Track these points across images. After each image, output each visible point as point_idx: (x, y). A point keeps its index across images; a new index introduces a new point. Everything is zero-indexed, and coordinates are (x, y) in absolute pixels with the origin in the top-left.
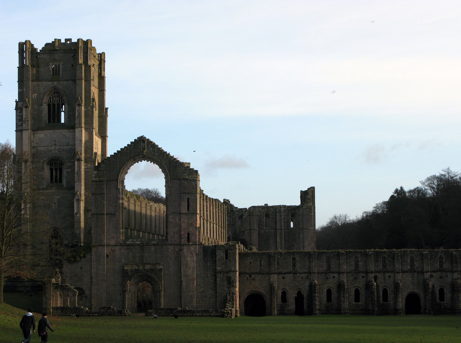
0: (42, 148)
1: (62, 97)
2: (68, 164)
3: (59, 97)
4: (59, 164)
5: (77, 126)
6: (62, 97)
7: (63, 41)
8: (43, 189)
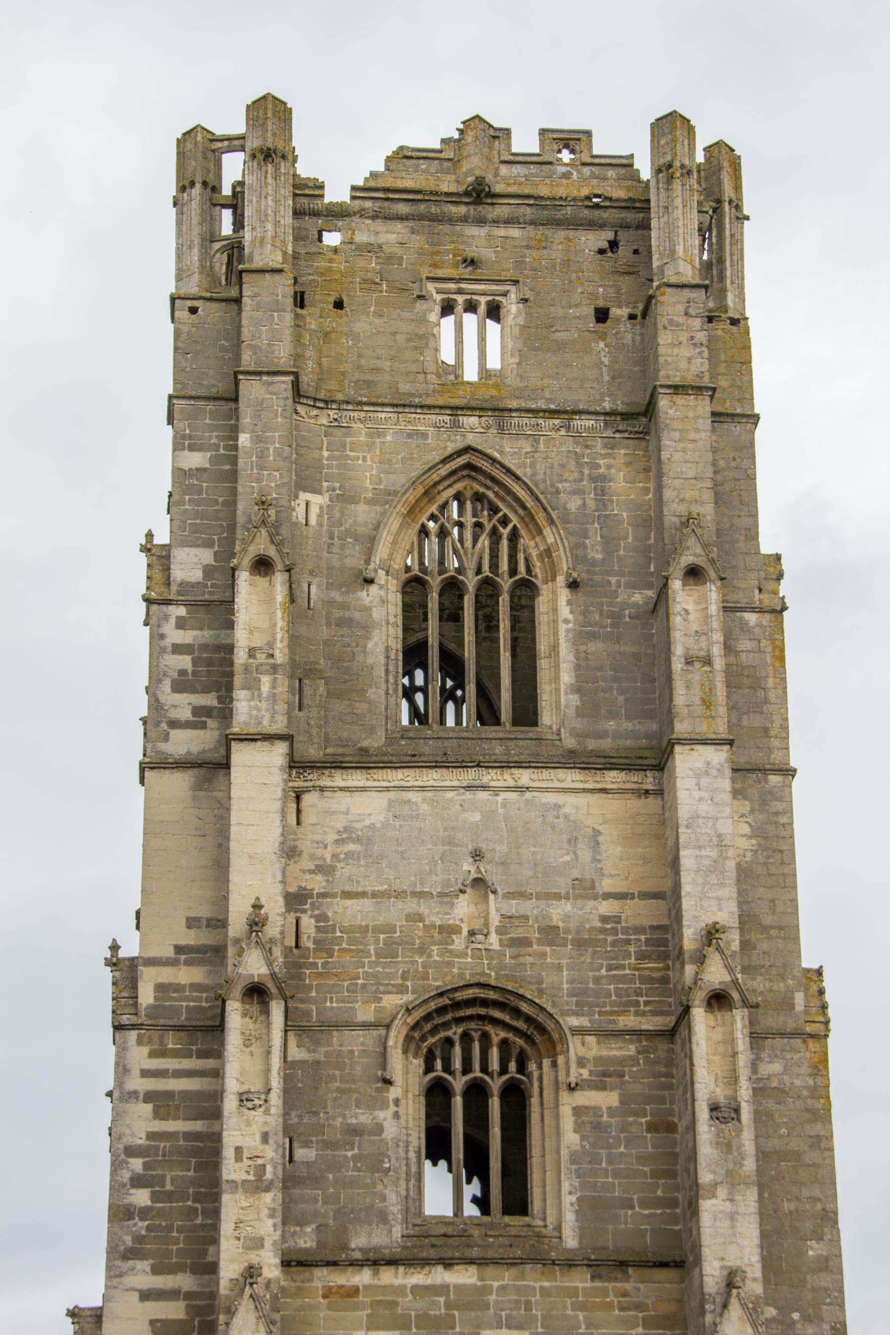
0: (366, 904)
1: (514, 536)
3: (495, 535)
5: (681, 728)
7: (525, 142)
8: (376, 1261)
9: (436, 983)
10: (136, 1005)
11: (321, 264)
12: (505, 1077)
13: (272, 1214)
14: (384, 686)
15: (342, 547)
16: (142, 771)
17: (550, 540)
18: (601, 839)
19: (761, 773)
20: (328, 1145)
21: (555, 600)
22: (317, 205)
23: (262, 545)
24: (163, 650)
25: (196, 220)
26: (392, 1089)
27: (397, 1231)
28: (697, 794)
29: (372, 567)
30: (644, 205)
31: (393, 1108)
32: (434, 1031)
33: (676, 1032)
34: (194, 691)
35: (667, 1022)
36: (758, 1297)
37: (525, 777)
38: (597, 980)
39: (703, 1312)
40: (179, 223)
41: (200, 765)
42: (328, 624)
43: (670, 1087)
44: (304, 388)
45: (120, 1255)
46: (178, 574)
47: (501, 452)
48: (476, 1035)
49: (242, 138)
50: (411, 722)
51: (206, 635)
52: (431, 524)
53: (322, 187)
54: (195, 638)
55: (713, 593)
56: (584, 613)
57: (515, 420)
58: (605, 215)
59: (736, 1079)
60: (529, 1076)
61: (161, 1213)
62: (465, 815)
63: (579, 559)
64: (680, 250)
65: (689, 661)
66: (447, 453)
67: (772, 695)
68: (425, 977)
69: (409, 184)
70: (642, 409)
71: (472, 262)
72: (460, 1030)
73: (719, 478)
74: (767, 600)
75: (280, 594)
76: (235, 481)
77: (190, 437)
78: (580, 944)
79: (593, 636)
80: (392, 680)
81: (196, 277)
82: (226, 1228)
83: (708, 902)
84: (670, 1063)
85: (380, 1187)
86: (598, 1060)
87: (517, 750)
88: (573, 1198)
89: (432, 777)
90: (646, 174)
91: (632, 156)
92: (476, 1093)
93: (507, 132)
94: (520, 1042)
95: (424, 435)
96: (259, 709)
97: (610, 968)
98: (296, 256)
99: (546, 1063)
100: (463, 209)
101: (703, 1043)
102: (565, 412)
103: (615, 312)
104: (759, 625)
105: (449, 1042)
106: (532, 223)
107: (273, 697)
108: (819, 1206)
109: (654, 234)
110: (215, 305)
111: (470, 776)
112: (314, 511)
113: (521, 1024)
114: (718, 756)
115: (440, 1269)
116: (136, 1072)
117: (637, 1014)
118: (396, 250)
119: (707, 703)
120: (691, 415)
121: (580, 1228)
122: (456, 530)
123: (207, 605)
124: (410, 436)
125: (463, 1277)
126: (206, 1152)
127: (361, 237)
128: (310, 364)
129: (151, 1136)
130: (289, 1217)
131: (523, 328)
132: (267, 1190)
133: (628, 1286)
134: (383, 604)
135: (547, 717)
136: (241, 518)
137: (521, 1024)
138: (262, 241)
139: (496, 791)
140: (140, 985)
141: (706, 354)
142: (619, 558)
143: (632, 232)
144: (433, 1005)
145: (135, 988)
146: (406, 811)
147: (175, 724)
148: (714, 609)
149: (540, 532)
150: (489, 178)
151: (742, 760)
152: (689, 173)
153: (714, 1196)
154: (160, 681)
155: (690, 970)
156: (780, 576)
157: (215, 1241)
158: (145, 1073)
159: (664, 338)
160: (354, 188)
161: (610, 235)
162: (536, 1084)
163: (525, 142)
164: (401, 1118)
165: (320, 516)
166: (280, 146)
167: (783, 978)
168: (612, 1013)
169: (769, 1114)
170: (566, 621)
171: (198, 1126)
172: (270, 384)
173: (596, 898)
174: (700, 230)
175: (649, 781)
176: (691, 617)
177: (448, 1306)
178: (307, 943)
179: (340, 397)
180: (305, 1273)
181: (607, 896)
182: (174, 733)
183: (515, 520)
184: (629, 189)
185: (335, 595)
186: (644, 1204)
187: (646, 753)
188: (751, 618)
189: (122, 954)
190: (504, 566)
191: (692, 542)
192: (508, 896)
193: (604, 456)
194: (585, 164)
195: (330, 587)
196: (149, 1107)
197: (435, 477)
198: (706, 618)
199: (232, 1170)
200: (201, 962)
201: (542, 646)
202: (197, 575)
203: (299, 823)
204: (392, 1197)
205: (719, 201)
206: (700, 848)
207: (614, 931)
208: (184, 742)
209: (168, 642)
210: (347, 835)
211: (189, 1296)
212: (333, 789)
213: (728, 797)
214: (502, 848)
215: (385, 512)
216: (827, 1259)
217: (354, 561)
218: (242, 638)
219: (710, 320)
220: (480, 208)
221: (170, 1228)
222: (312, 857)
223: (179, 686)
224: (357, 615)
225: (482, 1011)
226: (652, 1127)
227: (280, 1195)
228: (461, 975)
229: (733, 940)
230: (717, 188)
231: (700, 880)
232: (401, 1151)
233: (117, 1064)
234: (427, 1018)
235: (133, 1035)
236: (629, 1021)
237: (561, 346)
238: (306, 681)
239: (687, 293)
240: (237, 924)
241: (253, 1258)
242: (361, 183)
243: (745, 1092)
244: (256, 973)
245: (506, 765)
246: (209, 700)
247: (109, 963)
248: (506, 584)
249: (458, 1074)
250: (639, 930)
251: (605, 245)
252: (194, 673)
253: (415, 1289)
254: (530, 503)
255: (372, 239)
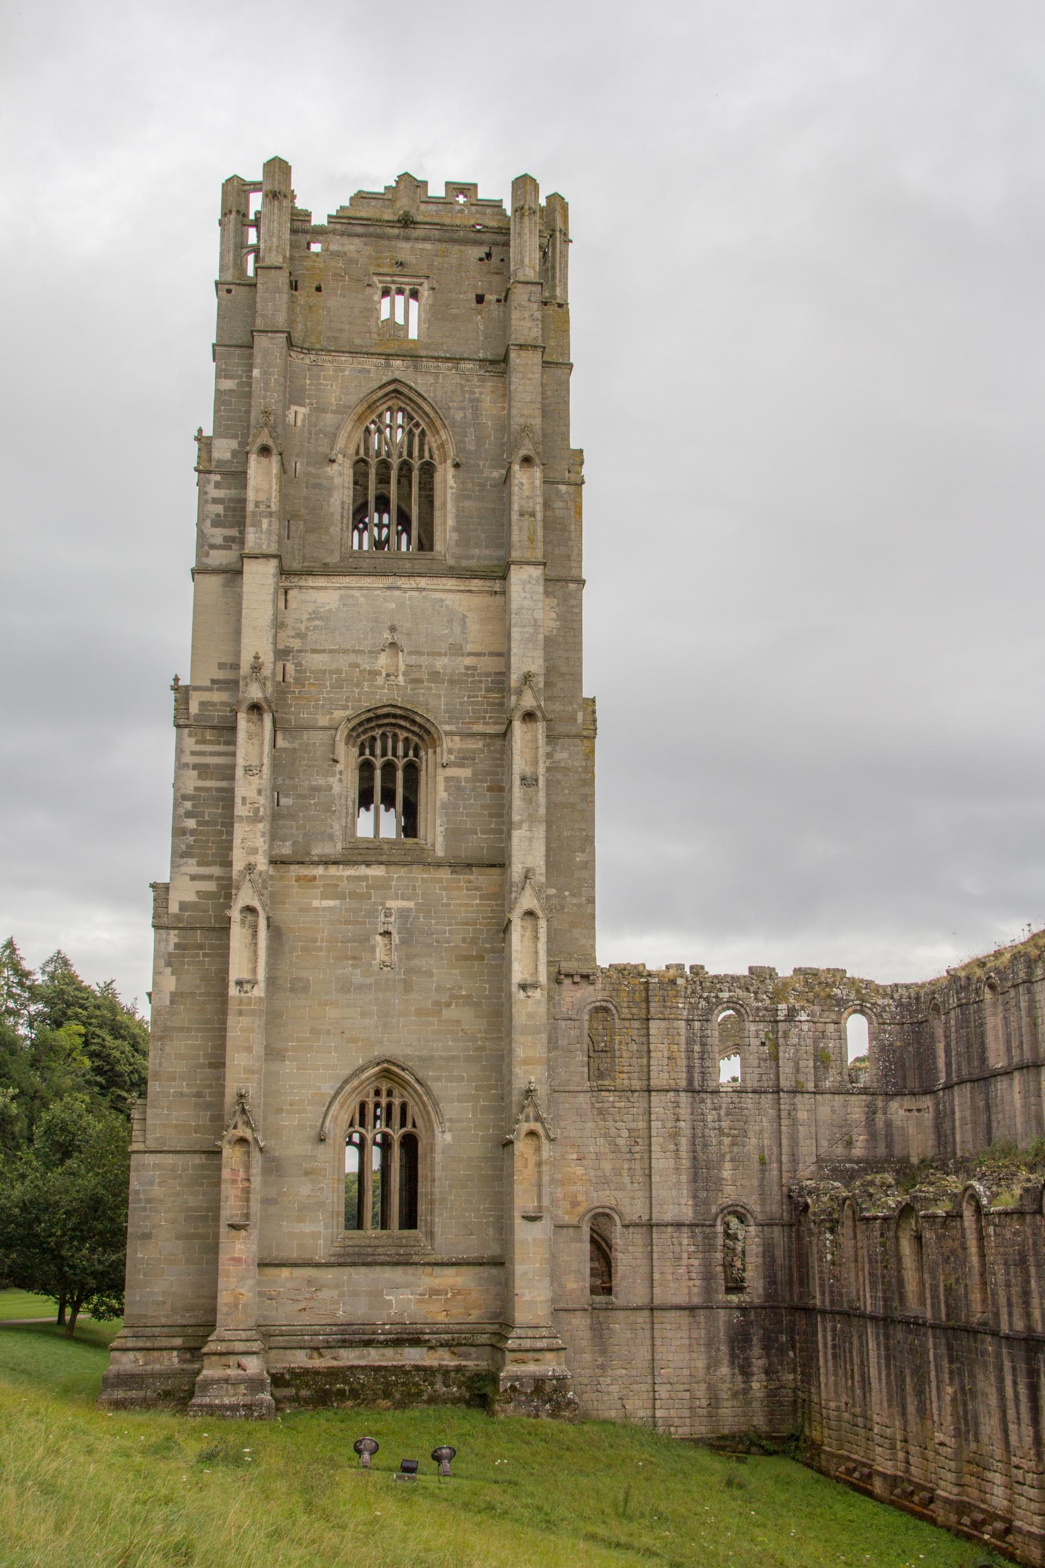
0: (325, 657)
1: (423, 433)
2: (457, 743)
4: (406, 740)
5: (515, 555)
6: (423, 433)
7: (436, 190)
8: (326, 863)
9: (366, 704)
10: (188, 713)
11: (308, 263)
12: (406, 759)
13: (263, 835)
14: (340, 526)
15: (317, 439)
16: (193, 574)
17: (444, 438)
18: (467, 620)
19: (564, 581)
20: (299, 796)
21: (445, 475)
22: (306, 226)
23: (265, 439)
24: (206, 501)
25: (232, 234)
26: (338, 765)
27: (339, 846)
28: (523, 595)
29: (334, 452)
30: (504, 231)
31: (338, 776)
32: (365, 732)
33: (505, 735)
34: (225, 527)
35: (500, 729)
36: (542, 884)
37: (423, 582)
38: (462, 703)
39: (511, 892)
40: (222, 236)
41: (227, 572)
42: (307, 487)
43: (502, 766)
44: (295, 341)
45: (179, 855)
46: (216, 455)
47: (415, 383)
48: (390, 735)
49: (260, 183)
50: (370, 547)
51: (232, 493)
52: (373, 426)
53: (309, 215)
54: (226, 494)
55: (537, 473)
56: (463, 483)
57: (425, 363)
58: (484, 237)
59: (537, 762)
60: (420, 759)
61: (202, 832)
62: (387, 605)
63: (460, 450)
64: (527, 260)
65: (522, 515)
66: (384, 381)
67: (573, 535)
68: (359, 701)
69: (364, 214)
70: (502, 358)
71: (401, 264)
72: (380, 732)
73: (547, 402)
74: (573, 477)
75: (275, 468)
76: (250, 398)
77: (225, 370)
78: (452, 682)
79: (467, 497)
80: (345, 522)
81: (231, 271)
82: (237, 842)
83: (526, 659)
84: (502, 752)
85: (330, 821)
86: (461, 750)
87: (418, 567)
88: (443, 829)
89: (367, 582)
90: (509, 213)
91: (501, 201)
92: (389, 768)
93: (425, 183)
94: (416, 739)
95: (369, 371)
96: (261, 539)
97: (469, 697)
98: (292, 258)
99: (430, 751)
100: (396, 231)
101: (519, 741)
102: (455, 359)
103: (488, 297)
104: (568, 492)
105: (374, 739)
106: (439, 240)
107: (269, 531)
108: (584, 833)
109: (512, 250)
110: (242, 288)
111: (390, 581)
112: (300, 417)
113: (416, 729)
114: (536, 572)
115: (363, 867)
116: (188, 752)
117: (484, 724)
118: (355, 256)
119: (531, 540)
120: (530, 362)
121: (446, 845)
122: (388, 431)
123: (233, 474)
124: (360, 372)
125: (377, 871)
126: (227, 799)
127: (334, 247)
128: (300, 326)
129: (196, 789)
130: (274, 836)
131: (432, 306)
132: (260, 821)
133: (472, 877)
134: (340, 476)
135: (438, 546)
136: (253, 421)
137: (416, 729)
138: (270, 250)
139: (405, 591)
140: (191, 702)
141: (540, 326)
142: (485, 450)
143: (500, 247)
144: (364, 717)
145: (188, 704)
146: (351, 601)
147: (212, 547)
148: (538, 482)
149: (438, 433)
150: (413, 212)
151: (553, 574)
152: (534, 212)
153: (521, 828)
154: (204, 520)
155: (513, 698)
156: (582, 463)
157: (231, 849)
158: (193, 753)
159: (515, 315)
160: (329, 216)
161: (487, 250)
162: (424, 764)
163: (436, 190)
164: (344, 782)
165: (303, 420)
166: (283, 190)
167: (571, 704)
168: (469, 723)
169: (559, 782)
170: (452, 488)
171: (224, 784)
172: (273, 338)
173: (463, 655)
174: (540, 247)
175: (497, 586)
176: (525, 487)
177: (367, 887)
178: (290, 679)
179: (318, 346)
180: (284, 867)
181: (470, 654)
182: (212, 552)
183: (423, 425)
184: (499, 221)
185: (311, 469)
186: (483, 832)
187: (496, 569)
188: (563, 488)
189: (180, 683)
190: (416, 453)
191: (526, 441)
192: (410, 653)
193: (478, 387)
194: (472, 205)
195: (308, 464)
196: (196, 772)
197: (375, 397)
198: (533, 488)
199: (240, 810)
200: (226, 689)
201: (437, 503)
202: (228, 456)
203: (286, 608)
204: (337, 827)
205: (554, 230)
206: (523, 627)
207: (473, 675)
208: (218, 558)
209: (210, 496)
210: (315, 615)
211: (218, 878)
212: (307, 588)
213: (541, 597)
214: (408, 625)
215: (342, 420)
216: (587, 863)
217: (324, 448)
218: (251, 495)
219: (545, 304)
220: (407, 230)
221: (208, 841)
222: (294, 628)
223: (216, 524)
224: (324, 482)
225: (393, 721)
226: (490, 789)
227: (268, 826)
228: (381, 700)
229: (541, 680)
230: (552, 221)
231: (522, 646)
232: (343, 801)
233: (177, 748)
234: (361, 724)
235: (186, 730)
236: (479, 728)
237: (455, 318)
238: (292, 522)
239: (530, 287)
240: (245, 669)
241: (252, 859)
242: (334, 213)
243: (541, 770)
244: (255, 697)
245: (411, 575)
246: (234, 532)
247: (173, 688)
248: (416, 464)
249: (379, 757)
250: (488, 675)
251: (484, 256)
252: (225, 516)
253: (349, 878)
254: (432, 414)
255: (340, 249)
